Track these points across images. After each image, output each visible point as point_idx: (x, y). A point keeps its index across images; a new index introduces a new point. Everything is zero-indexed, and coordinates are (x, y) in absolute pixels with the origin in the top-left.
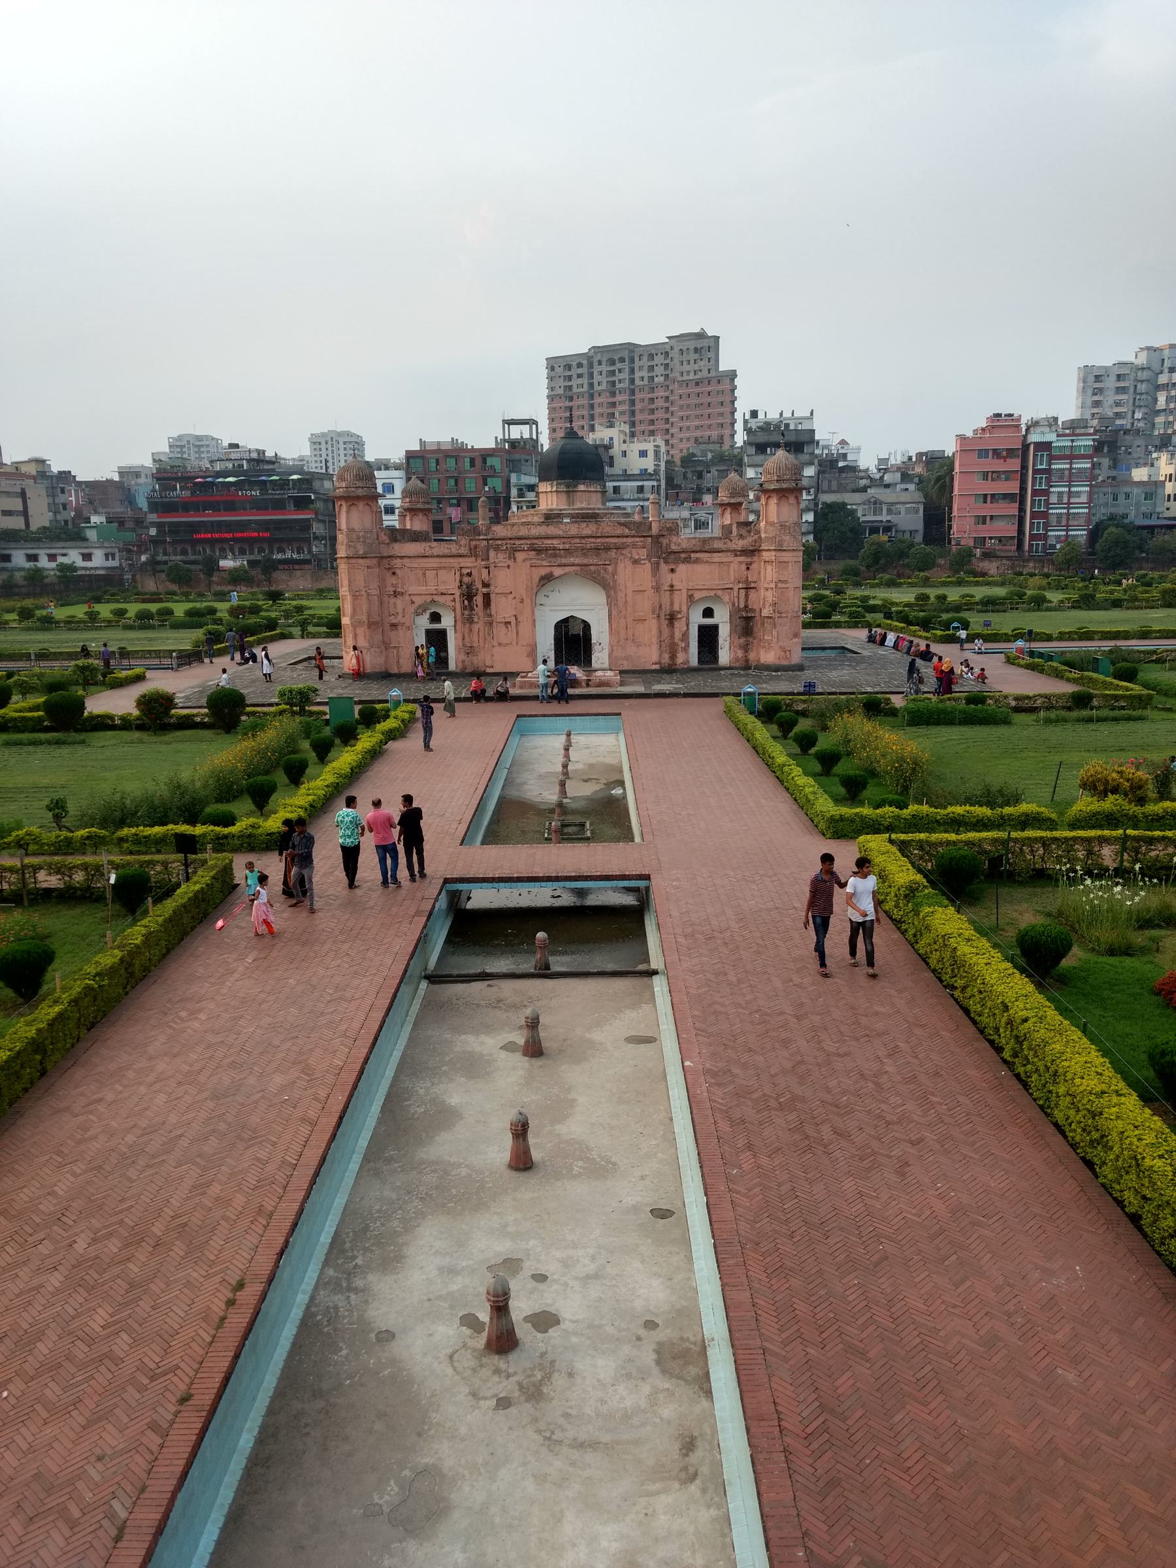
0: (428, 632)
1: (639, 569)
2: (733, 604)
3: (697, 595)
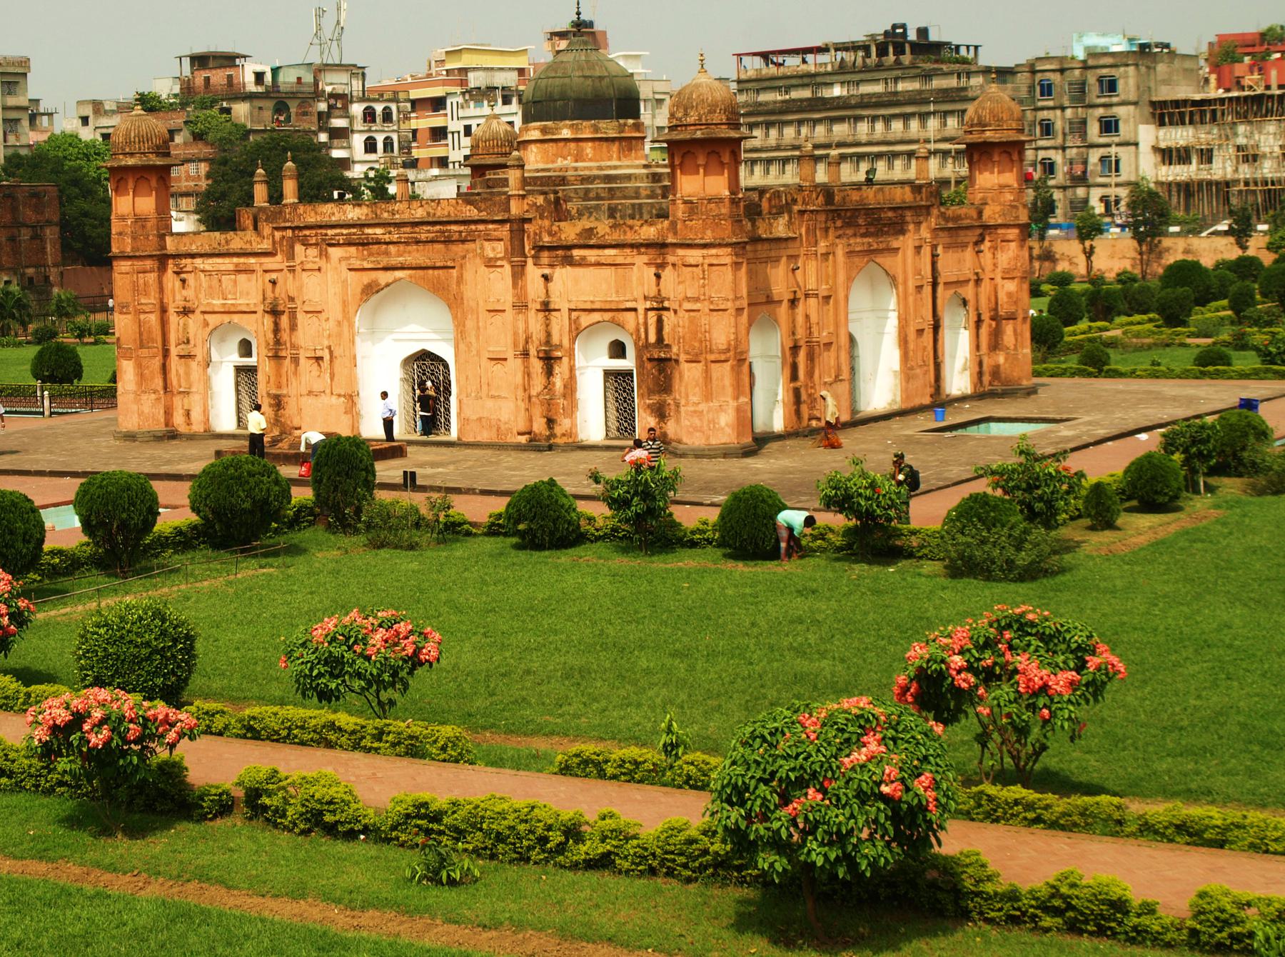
0: (239, 370)
1: (495, 274)
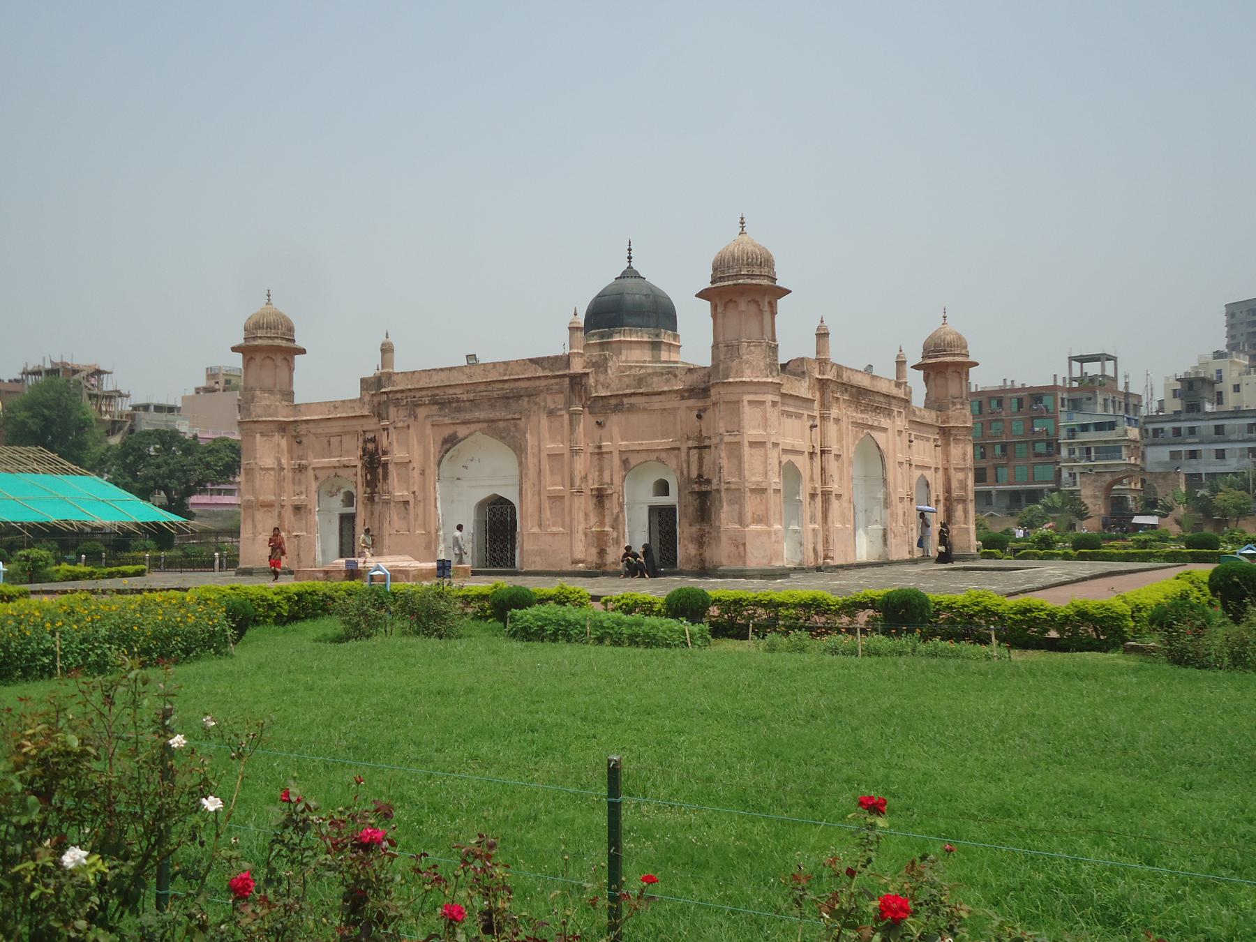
2: (682, 473)
3: (634, 460)
